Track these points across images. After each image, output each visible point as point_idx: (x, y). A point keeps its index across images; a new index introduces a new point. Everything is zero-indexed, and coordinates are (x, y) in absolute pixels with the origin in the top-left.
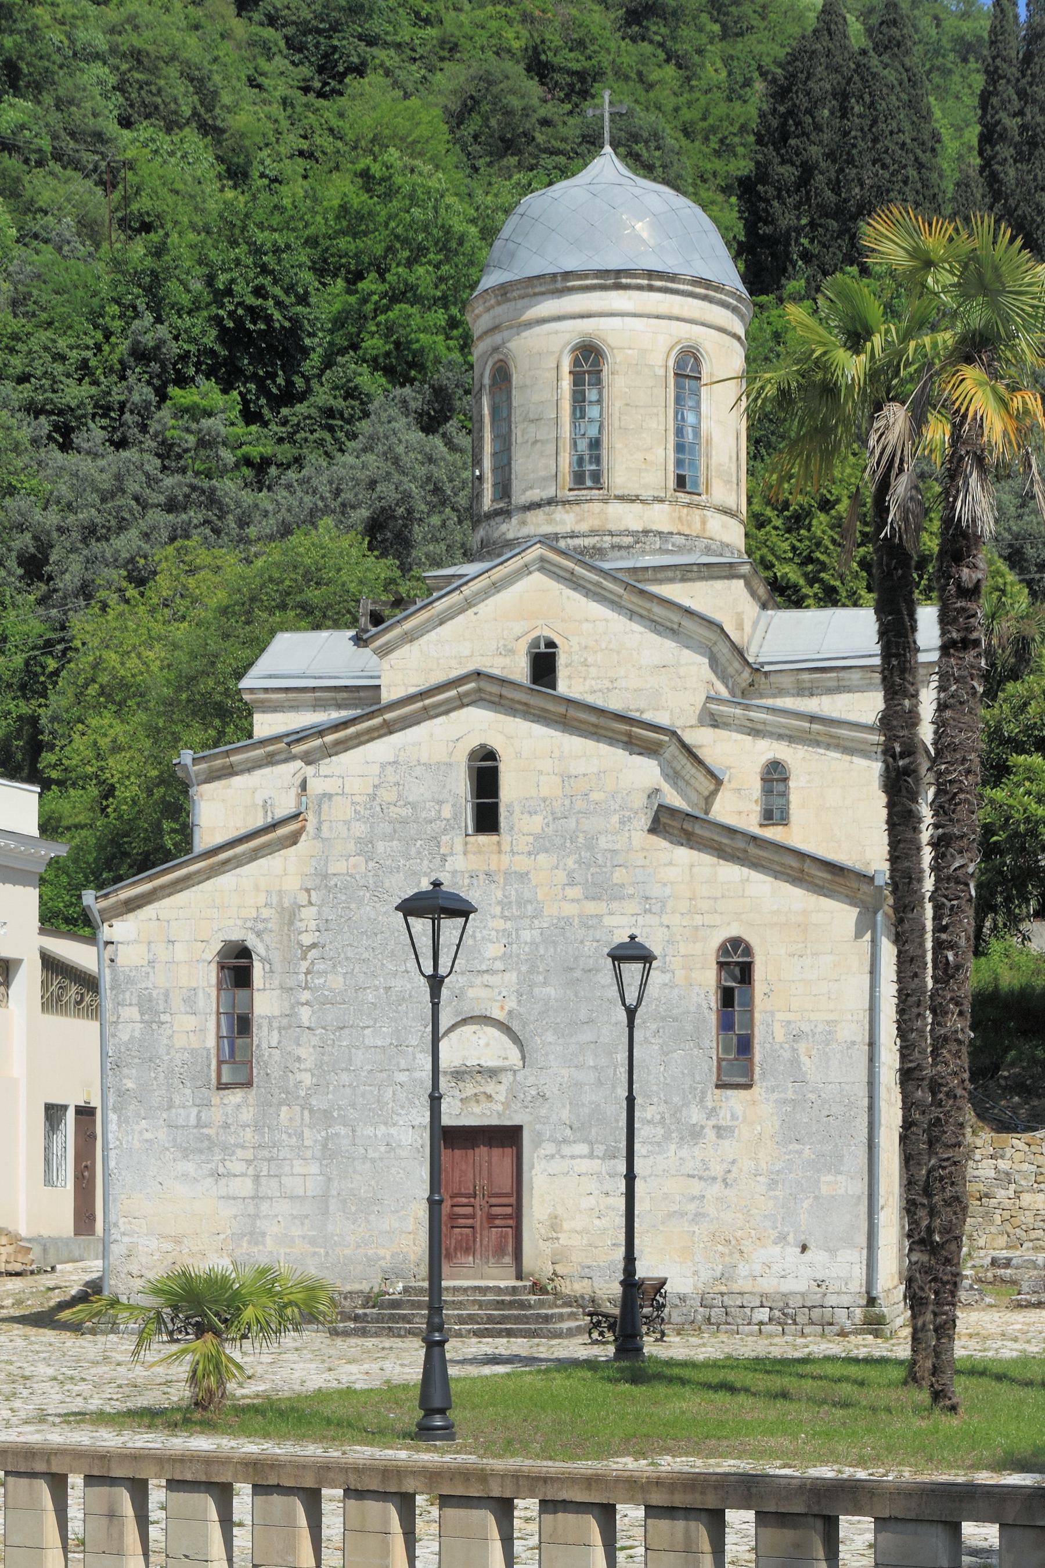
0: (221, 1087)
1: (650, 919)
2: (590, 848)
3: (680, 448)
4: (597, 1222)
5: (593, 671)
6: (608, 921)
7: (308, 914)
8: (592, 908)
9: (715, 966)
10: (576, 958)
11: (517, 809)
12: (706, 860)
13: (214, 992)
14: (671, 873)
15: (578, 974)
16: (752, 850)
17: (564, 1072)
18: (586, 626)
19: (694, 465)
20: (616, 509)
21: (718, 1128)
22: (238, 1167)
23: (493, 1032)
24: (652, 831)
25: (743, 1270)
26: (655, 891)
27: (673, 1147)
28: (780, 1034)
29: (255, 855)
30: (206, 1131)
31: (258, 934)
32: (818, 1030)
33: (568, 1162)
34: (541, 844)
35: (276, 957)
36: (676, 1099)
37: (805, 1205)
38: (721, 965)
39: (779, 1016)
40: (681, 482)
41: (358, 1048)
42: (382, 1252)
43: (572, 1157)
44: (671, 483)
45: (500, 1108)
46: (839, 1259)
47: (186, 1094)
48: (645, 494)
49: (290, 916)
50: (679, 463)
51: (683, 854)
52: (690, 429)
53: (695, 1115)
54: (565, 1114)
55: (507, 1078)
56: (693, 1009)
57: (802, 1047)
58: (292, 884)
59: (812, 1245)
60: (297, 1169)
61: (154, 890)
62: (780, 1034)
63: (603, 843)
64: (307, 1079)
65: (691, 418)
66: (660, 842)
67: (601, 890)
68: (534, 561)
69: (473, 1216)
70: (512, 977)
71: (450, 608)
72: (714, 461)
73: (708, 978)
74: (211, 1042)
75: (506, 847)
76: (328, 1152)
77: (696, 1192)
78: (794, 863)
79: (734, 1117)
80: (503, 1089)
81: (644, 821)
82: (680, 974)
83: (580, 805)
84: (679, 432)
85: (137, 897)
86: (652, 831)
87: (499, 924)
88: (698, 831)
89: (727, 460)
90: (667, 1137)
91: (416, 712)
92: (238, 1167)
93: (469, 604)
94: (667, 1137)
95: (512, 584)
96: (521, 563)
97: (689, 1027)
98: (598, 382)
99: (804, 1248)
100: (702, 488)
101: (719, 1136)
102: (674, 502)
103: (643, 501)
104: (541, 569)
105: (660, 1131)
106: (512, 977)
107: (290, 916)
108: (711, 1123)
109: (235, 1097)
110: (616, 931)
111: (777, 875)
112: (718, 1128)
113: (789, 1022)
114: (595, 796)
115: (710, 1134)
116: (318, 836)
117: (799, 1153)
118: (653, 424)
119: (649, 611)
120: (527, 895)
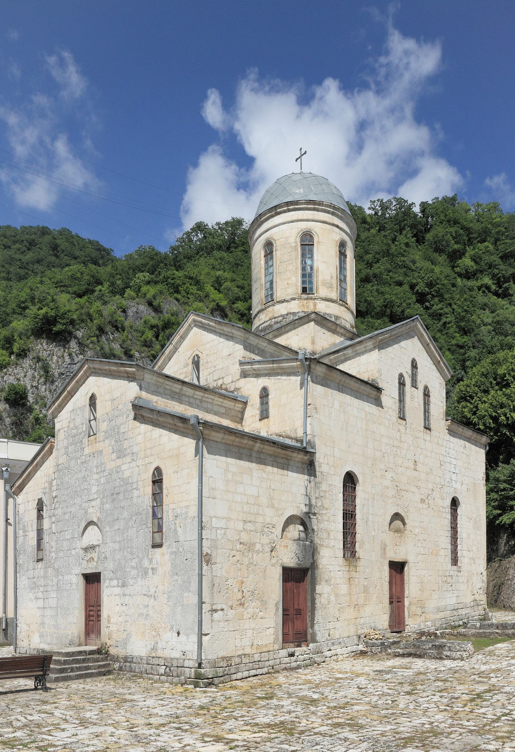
0: (38, 561)
1: (134, 464)
2: (118, 433)
3: (304, 276)
4: (120, 619)
5: (209, 364)
6: (123, 467)
7: (54, 483)
8: (119, 462)
9: (151, 483)
10: (114, 488)
11: (101, 420)
12: (149, 427)
13: (36, 520)
14: (140, 439)
15: (115, 496)
16: (161, 419)
17: (111, 545)
18: (208, 345)
19: (311, 282)
20: (278, 307)
21: (152, 569)
22: (40, 595)
23: (95, 527)
24: (135, 419)
25: (160, 646)
26: (135, 449)
27: (140, 580)
28: (171, 515)
29: (43, 461)
30: (35, 580)
31: (45, 494)
32: (183, 512)
33: (112, 589)
34: (108, 436)
35: (48, 504)
36: (141, 555)
37: (179, 610)
38: (154, 482)
39: (171, 506)
40: (304, 290)
41: (64, 540)
42: (70, 633)
43: (113, 587)
44: (300, 290)
45: (95, 564)
46: (190, 640)
47: (31, 565)
48: (288, 298)
49: (51, 484)
50: (303, 282)
51: (144, 428)
52: (309, 267)
53: (146, 563)
54: (112, 566)
55: (97, 549)
56: (145, 507)
57: (177, 522)
58: (51, 471)
59: (181, 632)
60: (52, 596)
61: (23, 480)
62: (171, 515)
63: (122, 430)
64: (53, 554)
65: (309, 262)
66: (137, 423)
67: (121, 454)
68: (191, 322)
69: (93, 616)
70: (98, 501)
71: (170, 352)
72: (320, 278)
73: (149, 489)
74: (36, 543)
75: (97, 440)
76: (59, 589)
77: (146, 604)
78: (170, 420)
79: (157, 564)
80: (96, 554)
81: (132, 415)
82: (142, 489)
83: (116, 413)
84: (304, 269)
85: (20, 484)
86: (135, 419)
87: (96, 476)
88: (144, 414)
89: (329, 278)
90: (138, 576)
91: (75, 385)
92: (40, 595)
93: (176, 349)
94: (138, 576)
95: (187, 335)
96: (188, 325)
97: (144, 517)
98: (272, 258)
99: (178, 634)
100: (314, 291)
101: (153, 574)
102: (300, 299)
103: (287, 301)
104: (195, 326)
105: (136, 572)
106: (98, 501)
107: (51, 484)
108: (151, 567)
109: (40, 564)
110: (125, 472)
111: (170, 430)
112: (152, 569)
113: (174, 509)
114: (120, 407)
115: (150, 571)
116: (57, 449)
117: (177, 580)
118: (291, 268)
119: (223, 330)
120: (102, 461)
